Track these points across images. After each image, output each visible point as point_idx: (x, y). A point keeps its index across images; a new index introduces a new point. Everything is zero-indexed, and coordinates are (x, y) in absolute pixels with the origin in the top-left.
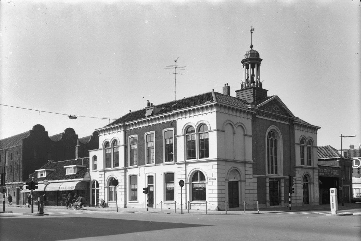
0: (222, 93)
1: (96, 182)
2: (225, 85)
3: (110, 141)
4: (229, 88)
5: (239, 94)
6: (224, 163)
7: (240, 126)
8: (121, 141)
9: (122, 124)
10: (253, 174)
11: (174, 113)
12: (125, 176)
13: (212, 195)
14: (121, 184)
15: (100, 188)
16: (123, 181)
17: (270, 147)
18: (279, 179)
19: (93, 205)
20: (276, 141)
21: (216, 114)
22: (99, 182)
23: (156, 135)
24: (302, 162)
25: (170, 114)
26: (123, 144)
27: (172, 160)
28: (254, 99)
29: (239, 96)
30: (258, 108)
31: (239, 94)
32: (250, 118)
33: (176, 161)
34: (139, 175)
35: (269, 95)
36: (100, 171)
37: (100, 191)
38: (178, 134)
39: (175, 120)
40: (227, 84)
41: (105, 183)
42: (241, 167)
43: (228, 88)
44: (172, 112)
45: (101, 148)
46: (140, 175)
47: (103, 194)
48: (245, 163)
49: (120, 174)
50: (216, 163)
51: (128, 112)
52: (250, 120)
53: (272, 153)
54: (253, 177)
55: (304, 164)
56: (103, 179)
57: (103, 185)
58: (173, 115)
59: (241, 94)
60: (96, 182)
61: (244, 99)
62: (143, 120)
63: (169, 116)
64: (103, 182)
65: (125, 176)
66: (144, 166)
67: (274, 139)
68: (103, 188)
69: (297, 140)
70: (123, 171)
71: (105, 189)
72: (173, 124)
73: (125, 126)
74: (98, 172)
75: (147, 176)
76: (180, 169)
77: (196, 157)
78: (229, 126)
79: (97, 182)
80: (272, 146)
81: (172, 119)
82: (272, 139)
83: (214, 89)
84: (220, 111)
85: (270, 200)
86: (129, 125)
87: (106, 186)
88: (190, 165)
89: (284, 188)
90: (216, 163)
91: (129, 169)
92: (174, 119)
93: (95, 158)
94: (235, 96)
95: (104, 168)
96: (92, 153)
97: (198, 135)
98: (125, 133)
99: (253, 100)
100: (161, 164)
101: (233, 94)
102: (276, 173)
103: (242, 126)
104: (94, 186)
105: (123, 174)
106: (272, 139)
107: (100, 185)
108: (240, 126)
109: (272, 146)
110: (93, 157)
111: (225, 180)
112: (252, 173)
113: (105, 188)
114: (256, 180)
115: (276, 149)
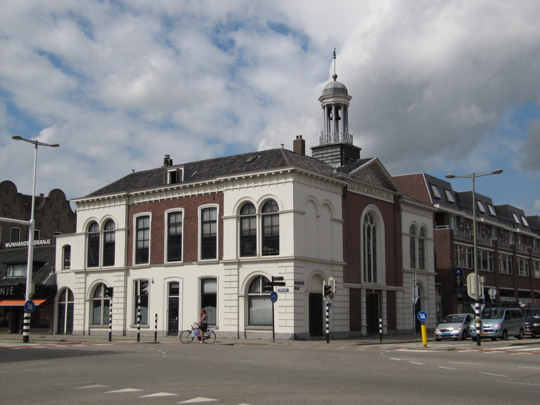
0: (293, 151)
1: (67, 290)
2: (298, 137)
3: (98, 222)
4: (303, 142)
5: (315, 153)
6: (302, 264)
7: (311, 201)
8: (120, 222)
9: (125, 193)
10: (344, 282)
11: (221, 180)
12: (126, 281)
13: (283, 316)
14: (118, 295)
15: (75, 302)
16: (122, 289)
17: (366, 240)
18: (380, 292)
19: (60, 331)
20: (374, 228)
21: (292, 185)
22: (74, 291)
23: (185, 214)
24: (413, 265)
25: (213, 181)
26: (124, 227)
27: (215, 257)
28: (342, 162)
29: (316, 157)
30: (352, 177)
31: (315, 153)
32: (431, 217)
33: (221, 257)
34: (151, 281)
35: (363, 155)
36: (77, 272)
37: (75, 307)
38: (226, 214)
39: (222, 192)
40: (301, 136)
41: (85, 293)
42: (325, 270)
43: (300, 143)
44: (217, 179)
45: (81, 232)
46: (153, 282)
47: (82, 312)
48: (332, 264)
49: (116, 279)
50: (292, 264)
51: (130, 172)
52: (431, 219)
53: (369, 248)
54: (344, 287)
55: (511, 273)
56: (83, 285)
57: (82, 296)
58: (218, 183)
59: (321, 152)
60: (67, 290)
61: (325, 162)
62: (162, 189)
63: (211, 183)
64: (83, 291)
65: (126, 281)
66: (162, 265)
67: (372, 226)
68: (82, 301)
69: (405, 228)
70: (123, 273)
71: (85, 304)
72: (219, 198)
73: (128, 197)
74: (74, 273)
75: (168, 283)
76: (228, 272)
77: (258, 253)
78: (310, 205)
79: (70, 291)
80: (369, 237)
81: (216, 190)
82: (369, 227)
83: (283, 145)
84: (314, 186)
85: (387, 323)
86: (136, 195)
87: (88, 298)
88: (244, 266)
89: (387, 305)
90: (292, 264)
91: (133, 269)
92: (220, 190)
93: (67, 249)
94: (311, 155)
95: (85, 267)
96: (61, 242)
97: (261, 219)
98: (129, 207)
99: (340, 164)
100: (194, 263)
101: (308, 152)
102: (375, 281)
103: (327, 205)
104: (62, 298)
105: (122, 278)
106: (369, 227)
107: (75, 296)
108: (311, 201)
109: (369, 237)
110: (63, 247)
111: (305, 291)
112: (434, 282)
113: (85, 301)
114: (347, 292)
115: (375, 241)
